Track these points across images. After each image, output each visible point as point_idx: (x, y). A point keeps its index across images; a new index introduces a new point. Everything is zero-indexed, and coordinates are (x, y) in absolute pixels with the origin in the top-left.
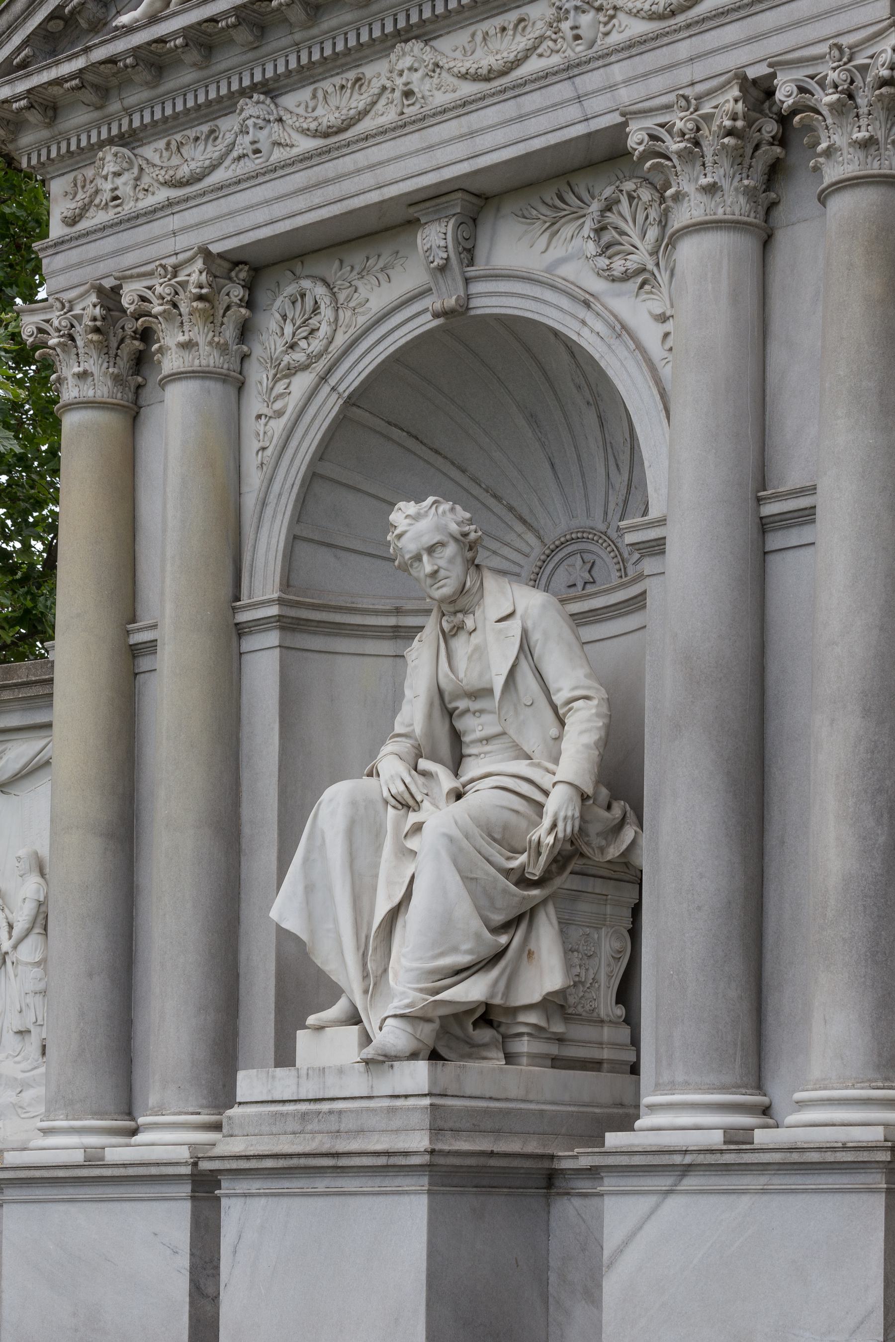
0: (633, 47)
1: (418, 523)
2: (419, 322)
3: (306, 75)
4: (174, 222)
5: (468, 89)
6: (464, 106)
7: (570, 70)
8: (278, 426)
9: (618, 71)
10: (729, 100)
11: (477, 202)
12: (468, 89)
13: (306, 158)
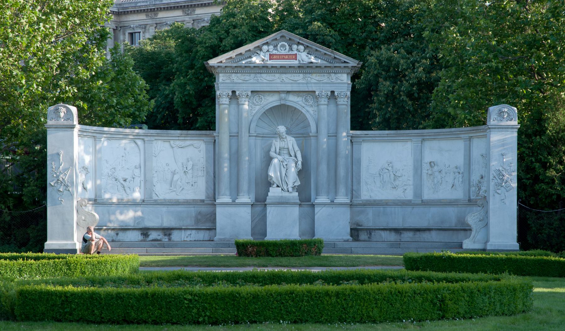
0: (315, 83)
1: (282, 129)
2: (277, 103)
3: (267, 73)
4: (244, 85)
5: (291, 81)
6: (292, 83)
7: (307, 83)
8: (254, 112)
9: (313, 85)
10: (329, 93)
11: (288, 92)
12: (291, 81)
13: (266, 83)
